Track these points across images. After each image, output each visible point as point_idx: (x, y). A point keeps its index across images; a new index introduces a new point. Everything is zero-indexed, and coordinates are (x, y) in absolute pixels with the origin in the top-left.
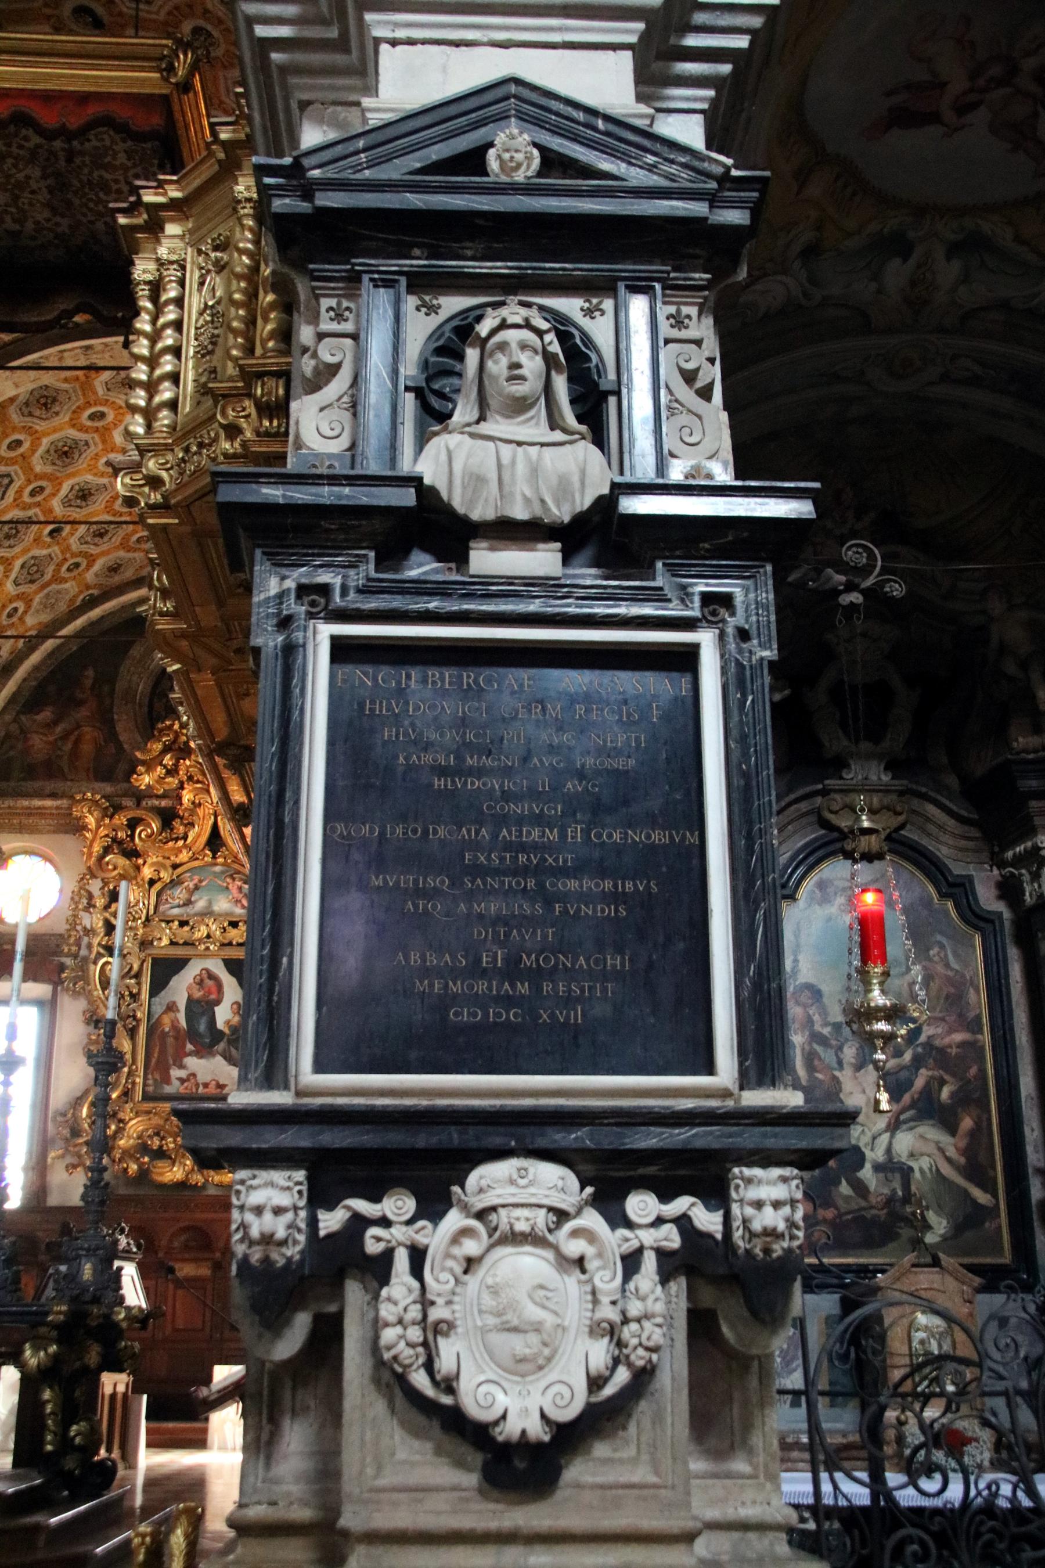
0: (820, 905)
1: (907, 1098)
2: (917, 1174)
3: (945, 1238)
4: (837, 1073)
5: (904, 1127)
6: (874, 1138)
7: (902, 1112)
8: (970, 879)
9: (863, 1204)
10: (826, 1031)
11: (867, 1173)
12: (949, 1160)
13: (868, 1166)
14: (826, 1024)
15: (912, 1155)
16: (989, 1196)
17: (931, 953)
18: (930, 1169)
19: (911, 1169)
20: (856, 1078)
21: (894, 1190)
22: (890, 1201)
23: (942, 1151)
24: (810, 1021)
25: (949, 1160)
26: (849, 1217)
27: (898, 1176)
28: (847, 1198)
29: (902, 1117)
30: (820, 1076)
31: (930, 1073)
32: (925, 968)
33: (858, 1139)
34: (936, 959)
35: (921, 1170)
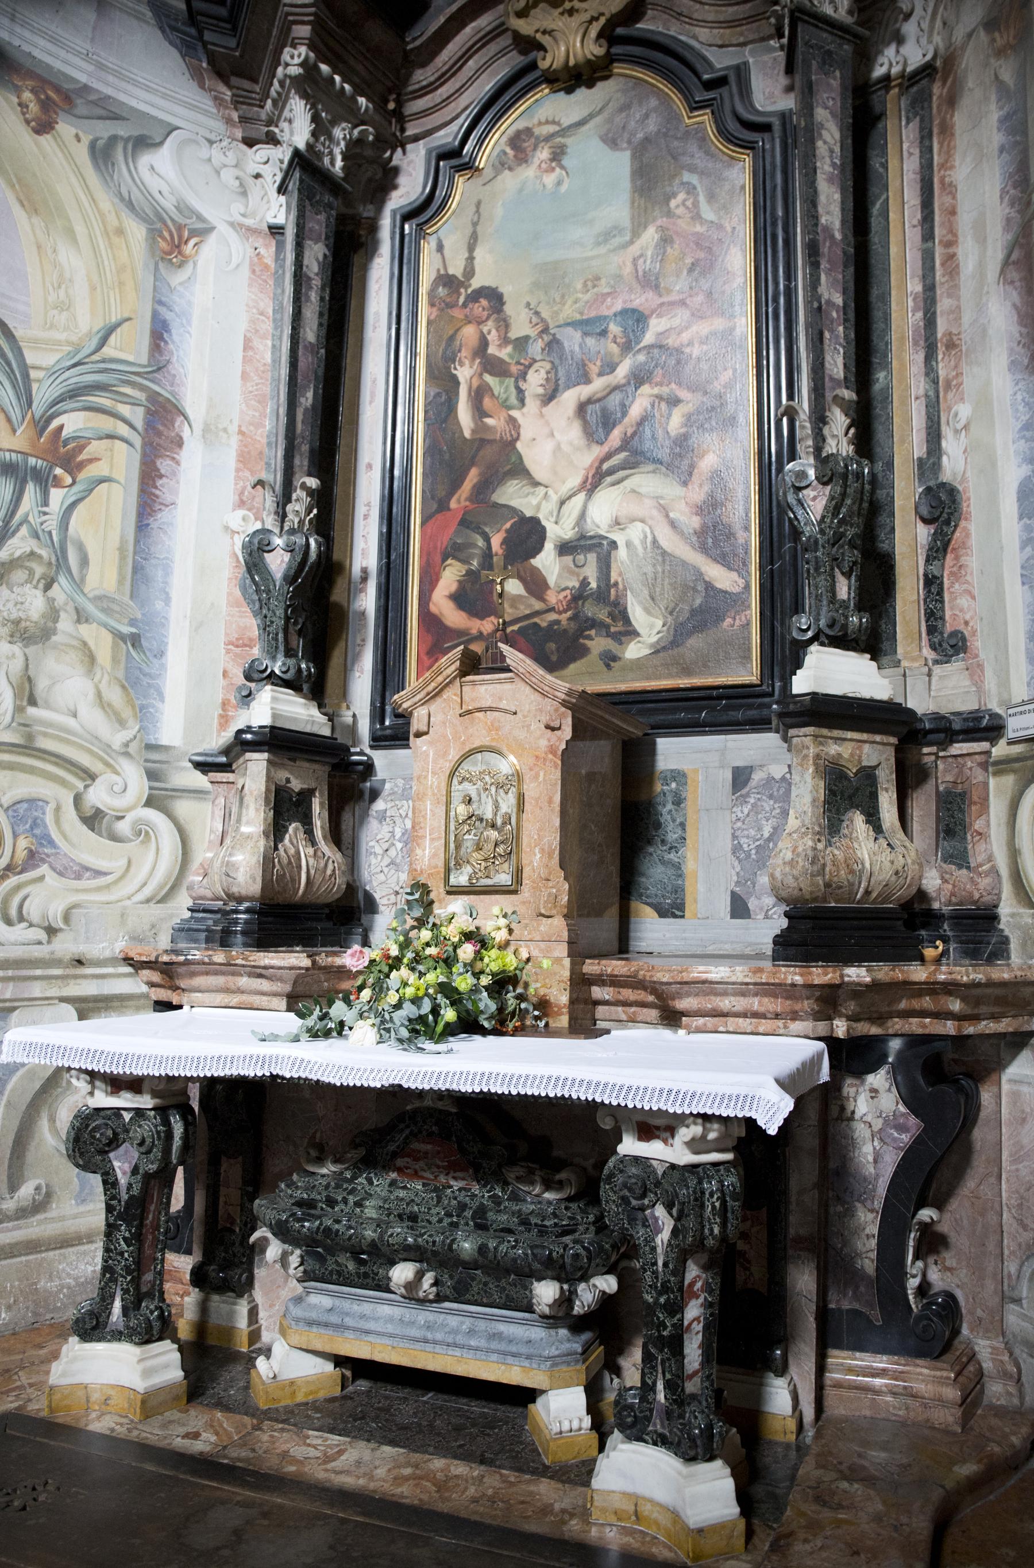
0: (510, 169)
1: (616, 436)
2: (622, 553)
3: (658, 650)
4: (514, 413)
5: (609, 479)
6: (562, 503)
7: (608, 456)
8: (742, 72)
9: (538, 606)
10: (504, 353)
11: (547, 561)
12: (673, 524)
13: (549, 546)
14: (505, 341)
15: (617, 523)
16: (734, 575)
17: (673, 203)
18: (644, 540)
19: (614, 544)
20: (542, 415)
21: (584, 583)
22: (579, 596)
23: (665, 511)
24: (484, 343)
25: (673, 524)
26: (515, 627)
27: (592, 557)
28: (516, 600)
29: (605, 466)
30: (489, 421)
31: (656, 391)
32: (662, 229)
33: (538, 507)
34: (680, 211)
35: (629, 544)
